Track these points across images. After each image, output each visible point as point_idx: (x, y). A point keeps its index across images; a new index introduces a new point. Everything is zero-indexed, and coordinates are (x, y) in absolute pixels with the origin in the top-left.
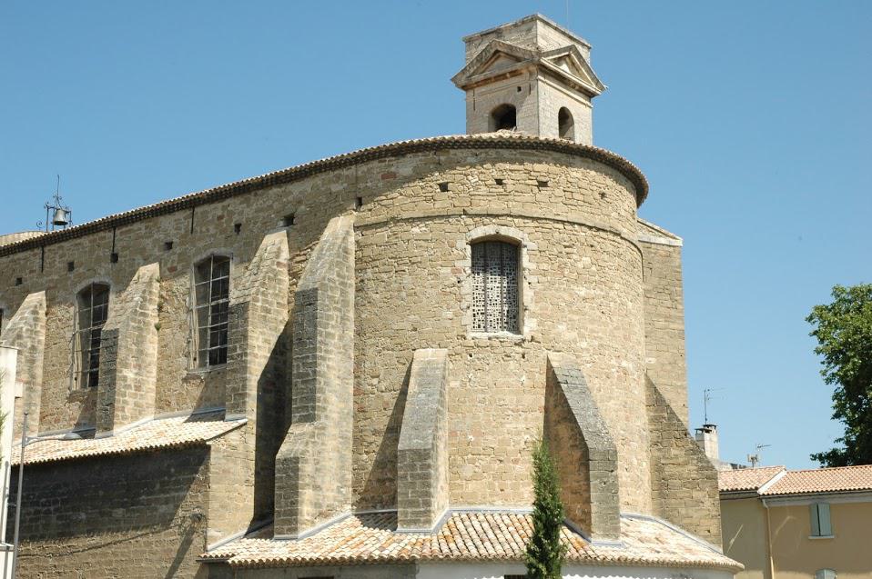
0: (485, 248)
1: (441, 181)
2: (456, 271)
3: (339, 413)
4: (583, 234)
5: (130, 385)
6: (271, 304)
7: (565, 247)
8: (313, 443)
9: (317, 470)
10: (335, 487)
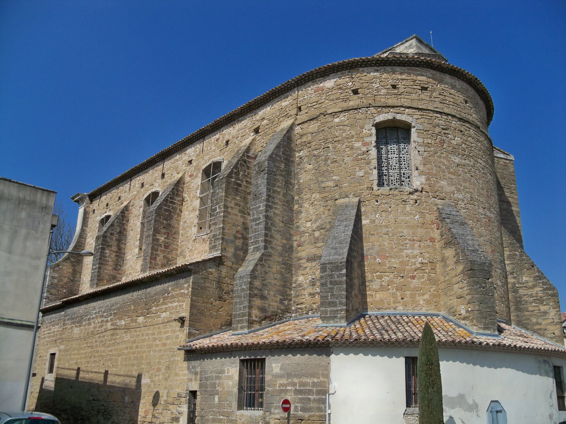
0: (386, 132)
1: (354, 88)
2: (365, 144)
3: (282, 246)
4: (455, 123)
5: (161, 245)
6: (242, 181)
7: (443, 129)
8: (261, 265)
9: (264, 285)
10: (278, 299)
